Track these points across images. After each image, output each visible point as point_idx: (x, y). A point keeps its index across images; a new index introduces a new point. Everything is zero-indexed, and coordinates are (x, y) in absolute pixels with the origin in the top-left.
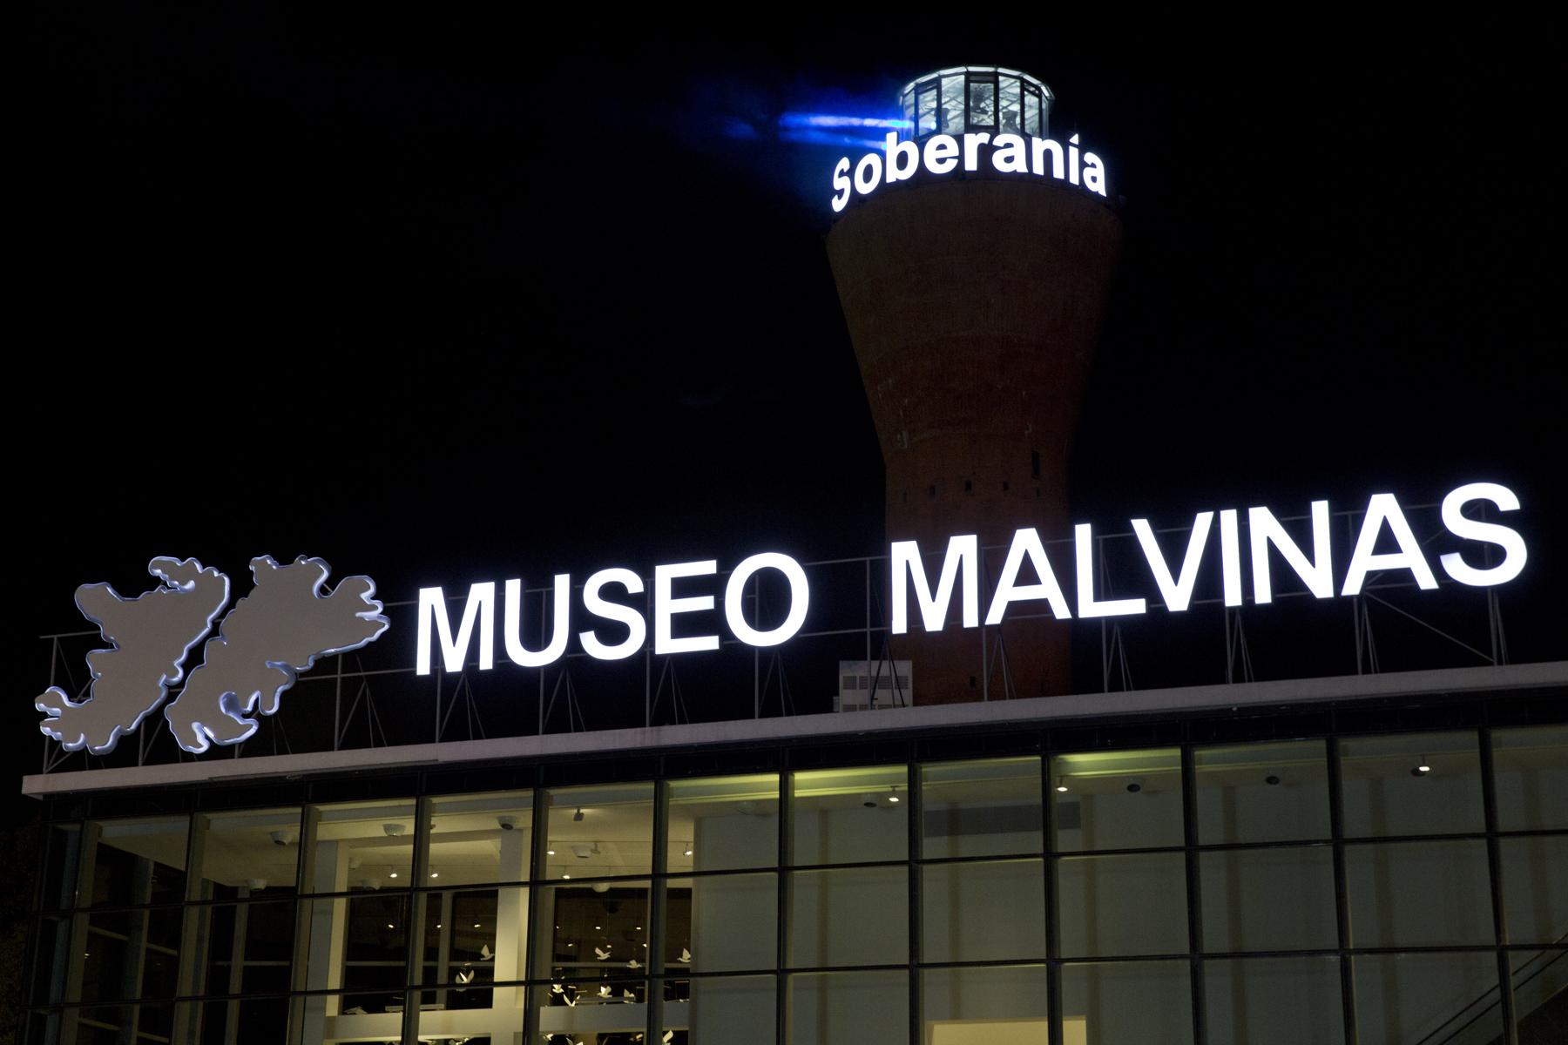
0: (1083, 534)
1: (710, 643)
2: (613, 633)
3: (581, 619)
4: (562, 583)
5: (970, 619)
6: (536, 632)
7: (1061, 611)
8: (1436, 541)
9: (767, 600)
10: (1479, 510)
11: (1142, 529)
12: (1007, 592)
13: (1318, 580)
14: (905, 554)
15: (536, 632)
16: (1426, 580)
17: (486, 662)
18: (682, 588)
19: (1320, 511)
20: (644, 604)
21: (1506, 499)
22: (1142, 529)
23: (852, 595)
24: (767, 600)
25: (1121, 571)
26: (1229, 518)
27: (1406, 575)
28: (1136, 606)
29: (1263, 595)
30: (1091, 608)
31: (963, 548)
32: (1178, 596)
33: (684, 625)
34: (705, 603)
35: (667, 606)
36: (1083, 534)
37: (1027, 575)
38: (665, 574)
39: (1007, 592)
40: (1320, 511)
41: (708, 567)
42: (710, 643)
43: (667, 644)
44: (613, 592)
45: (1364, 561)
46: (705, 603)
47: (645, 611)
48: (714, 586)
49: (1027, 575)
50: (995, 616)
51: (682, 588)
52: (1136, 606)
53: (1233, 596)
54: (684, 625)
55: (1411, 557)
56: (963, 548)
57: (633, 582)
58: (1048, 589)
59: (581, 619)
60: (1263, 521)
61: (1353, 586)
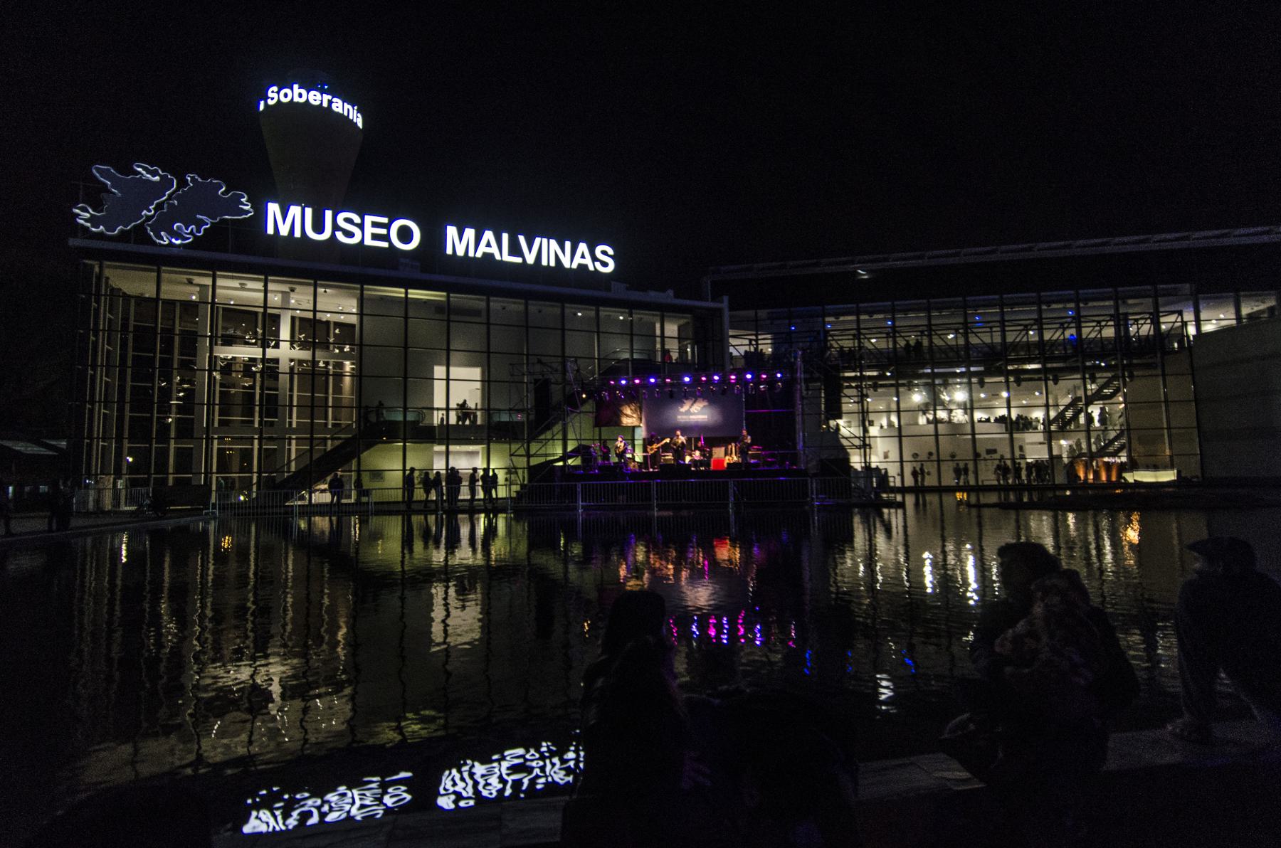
0: (505, 237)
1: (385, 245)
2: (350, 234)
3: (336, 227)
4: (329, 214)
5: (471, 254)
6: (319, 227)
7: (498, 257)
8: (594, 259)
9: (405, 235)
10: (604, 253)
11: (522, 239)
12: (482, 249)
14: (452, 231)
15: (319, 227)
16: (591, 268)
17: (298, 234)
18: (375, 225)
19: (568, 245)
21: (611, 252)
22: (522, 239)
23: (434, 239)
24: (405, 235)
25: (515, 249)
26: (545, 240)
27: (586, 266)
28: (519, 260)
29: (553, 264)
30: (507, 258)
31: (470, 233)
32: (530, 259)
34: (384, 231)
35: (369, 230)
36: (505, 237)
37: (488, 245)
38: (369, 219)
39: (482, 249)
40: (568, 245)
41: (385, 220)
42: (385, 245)
43: (369, 242)
46: (384, 231)
47: (362, 230)
48: (388, 226)
49: (488, 245)
50: (479, 255)
51: (375, 225)
52: (519, 260)
53: (544, 263)
55: (588, 261)
56: (470, 233)
57: (357, 219)
58: (494, 250)
60: (554, 244)
61: (575, 266)
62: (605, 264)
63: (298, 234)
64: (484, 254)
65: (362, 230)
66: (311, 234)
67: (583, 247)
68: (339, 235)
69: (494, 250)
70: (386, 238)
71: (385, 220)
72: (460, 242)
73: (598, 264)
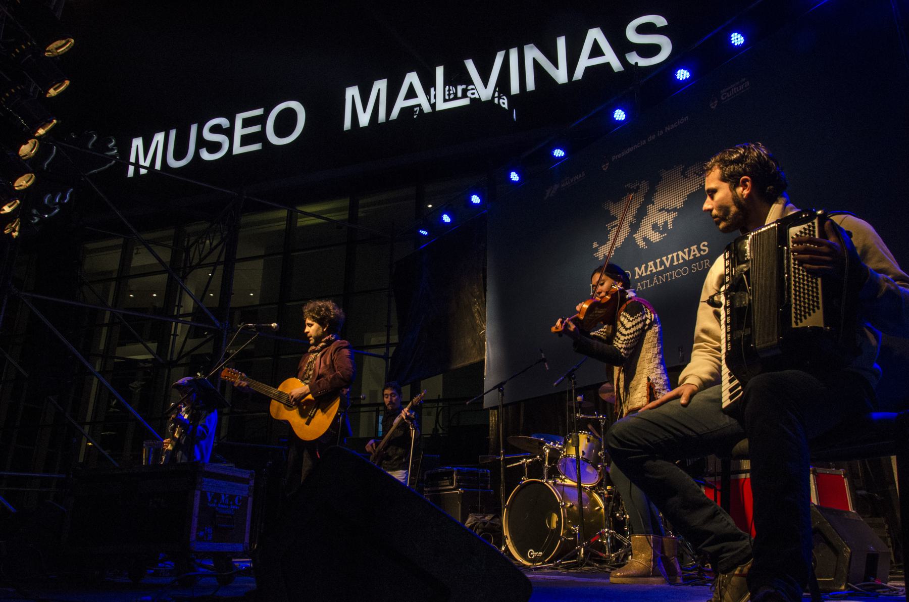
2: (214, 147)
8: (622, 47)
9: (285, 123)
12: (401, 103)
13: (560, 75)
16: (616, 65)
17: (158, 166)
18: (247, 123)
19: (561, 42)
20: (229, 133)
21: (660, 21)
24: (285, 123)
27: (607, 65)
29: (531, 85)
33: (246, 140)
34: (256, 129)
35: (239, 132)
37: (411, 94)
40: (561, 42)
41: (259, 112)
43: (238, 149)
44: (216, 129)
45: (585, 62)
46: (256, 129)
47: (229, 137)
51: (247, 123)
54: (246, 140)
55: (610, 57)
59: (201, 143)
60: (532, 53)
61: (579, 74)
62: (650, 50)
63: (158, 166)
64: (403, 110)
65: (229, 137)
66: (174, 164)
67: (595, 34)
68: (206, 155)
69: (421, 99)
70: (260, 137)
71: (259, 112)
72: (362, 107)
73: (633, 58)
